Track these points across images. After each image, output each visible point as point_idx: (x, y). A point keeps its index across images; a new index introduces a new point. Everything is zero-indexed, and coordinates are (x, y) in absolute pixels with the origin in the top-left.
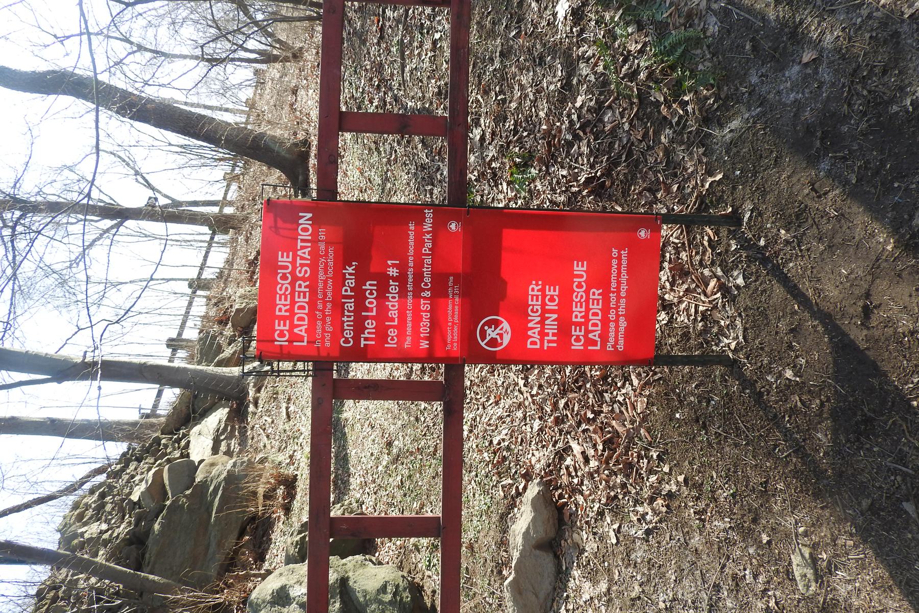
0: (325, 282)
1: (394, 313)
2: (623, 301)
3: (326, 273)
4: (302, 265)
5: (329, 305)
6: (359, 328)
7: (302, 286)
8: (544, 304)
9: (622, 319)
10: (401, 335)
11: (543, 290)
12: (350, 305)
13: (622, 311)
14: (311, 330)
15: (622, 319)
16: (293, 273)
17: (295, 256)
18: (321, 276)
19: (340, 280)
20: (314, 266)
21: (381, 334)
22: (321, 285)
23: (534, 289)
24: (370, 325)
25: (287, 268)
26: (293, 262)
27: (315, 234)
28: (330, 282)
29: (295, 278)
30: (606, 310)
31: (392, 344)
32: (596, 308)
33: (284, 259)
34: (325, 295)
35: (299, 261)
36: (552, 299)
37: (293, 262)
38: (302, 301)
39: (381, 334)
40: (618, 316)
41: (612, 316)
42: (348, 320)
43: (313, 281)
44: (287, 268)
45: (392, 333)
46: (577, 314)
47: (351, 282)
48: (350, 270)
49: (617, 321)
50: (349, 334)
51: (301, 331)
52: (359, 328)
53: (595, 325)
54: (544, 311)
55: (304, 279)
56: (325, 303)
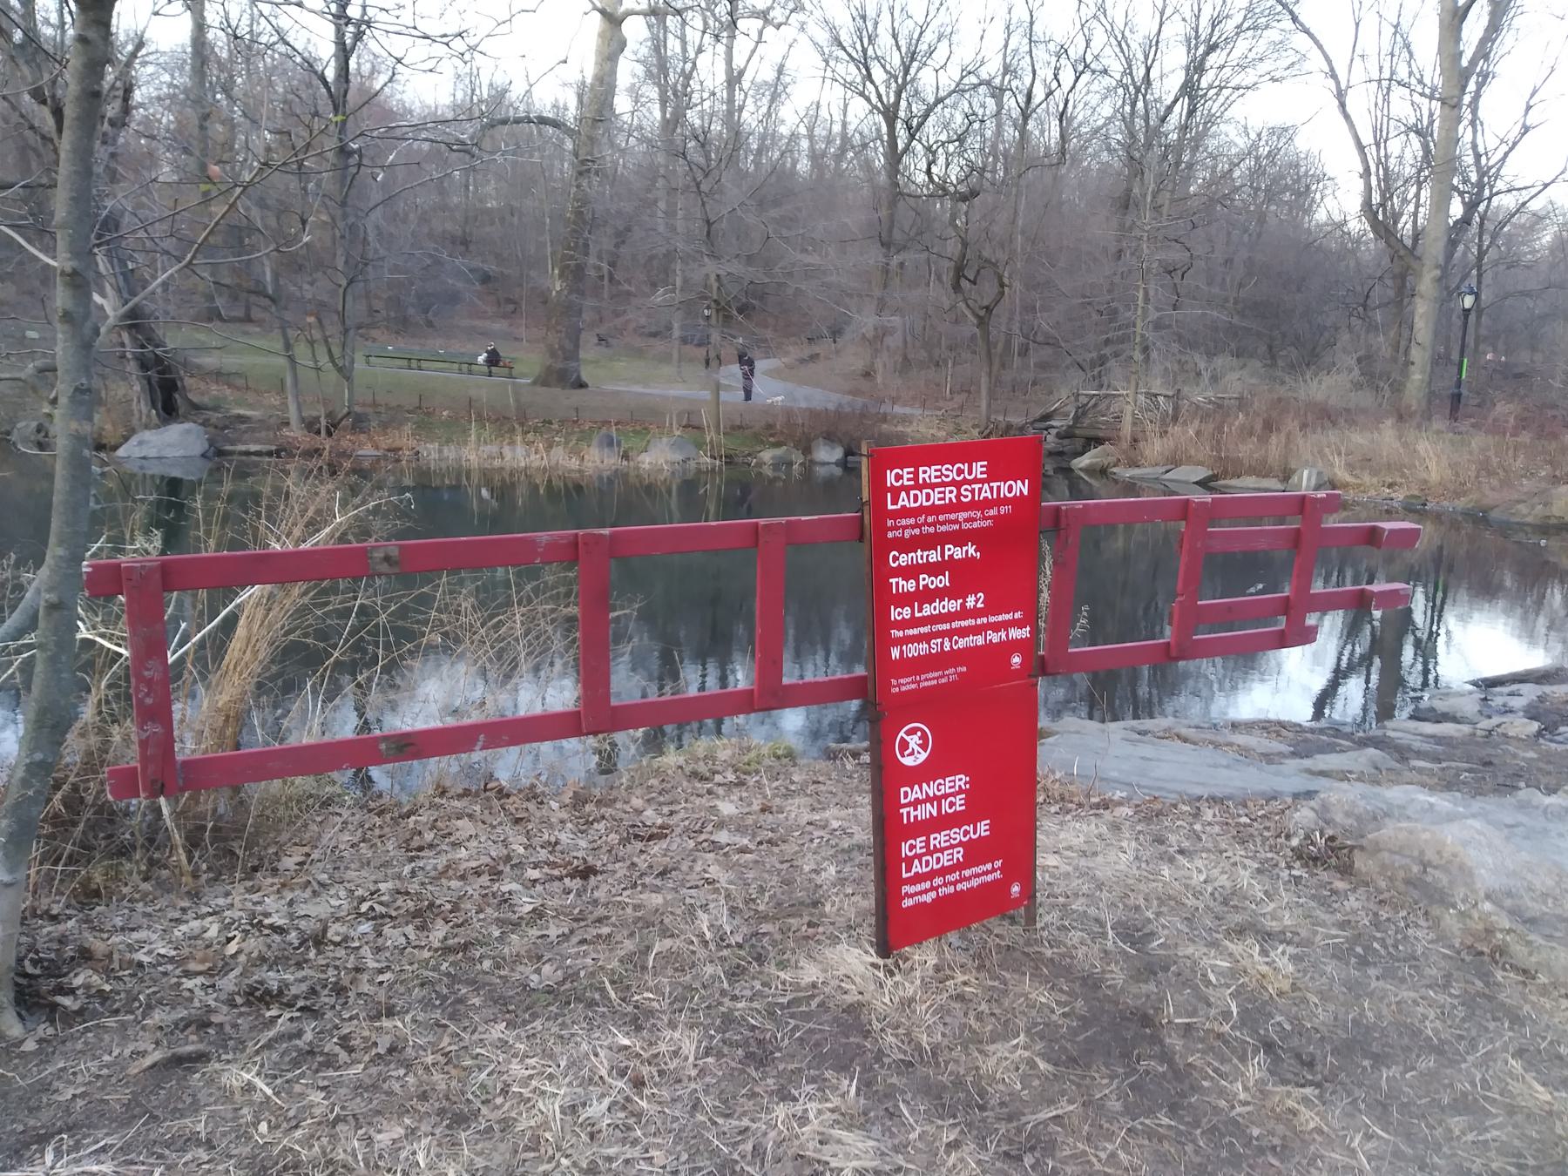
0: (956, 522)
1: (928, 610)
2: (951, 890)
3: (966, 520)
4: (973, 491)
5: (932, 530)
7: (951, 495)
8: (946, 796)
9: (933, 895)
10: (903, 625)
11: (961, 791)
12: (934, 556)
13: (942, 891)
15: (933, 895)
16: (965, 481)
17: (982, 481)
18: (963, 515)
19: (959, 539)
20: (973, 505)
21: (905, 599)
22: (953, 516)
23: (961, 780)
24: (910, 586)
25: (970, 473)
26: (976, 481)
28: (957, 527)
29: (958, 485)
30: (944, 871)
32: (945, 860)
33: (979, 468)
34: (942, 524)
35: (976, 487)
36: (952, 804)
37: (976, 481)
38: (935, 497)
39: (905, 599)
40: (936, 889)
41: (938, 881)
43: (958, 506)
44: (970, 473)
46: (939, 839)
47: (958, 553)
48: (971, 551)
49: (932, 888)
53: (927, 863)
54: (938, 799)
55: (959, 495)
56: (933, 524)
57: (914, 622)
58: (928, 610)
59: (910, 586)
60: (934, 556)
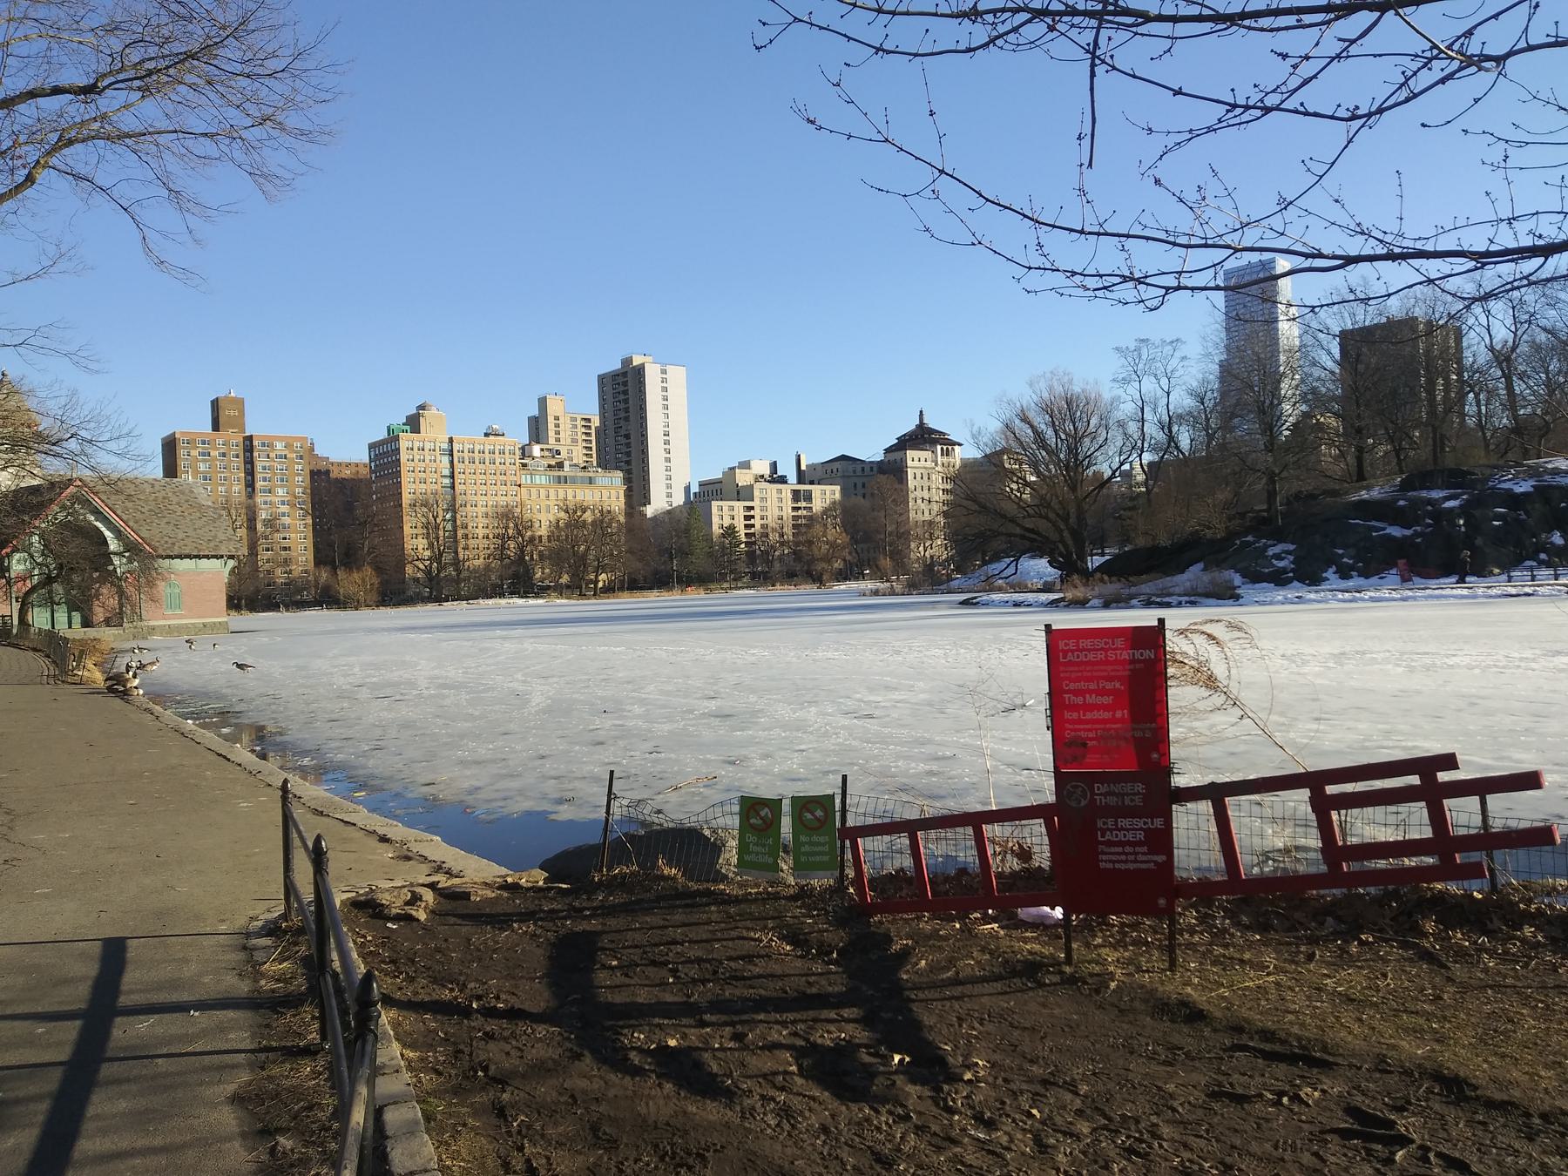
1: (1089, 716)
6: (1076, 693)
7: (1101, 656)
10: (1073, 722)
12: (1093, 686)
14: (1070, 663)
19: (1110, 679)
21: (1074, 708)
24: (1079, 700)
27: (1139, 661)
29: (1106, 650)
31: (1067, 715)
38: (1091, 657)
39: (1074, 708)
42: (1082, 685)
43: (1107, 662)
45: (1075, 715)
47: (1109, 686)
50: (1072, 686)
51: (1070, 657)
52: (1076, 693)
57: (1080, 721)
58: (1089, 716)
59: (1079, 700)
60: (1093, 686)
